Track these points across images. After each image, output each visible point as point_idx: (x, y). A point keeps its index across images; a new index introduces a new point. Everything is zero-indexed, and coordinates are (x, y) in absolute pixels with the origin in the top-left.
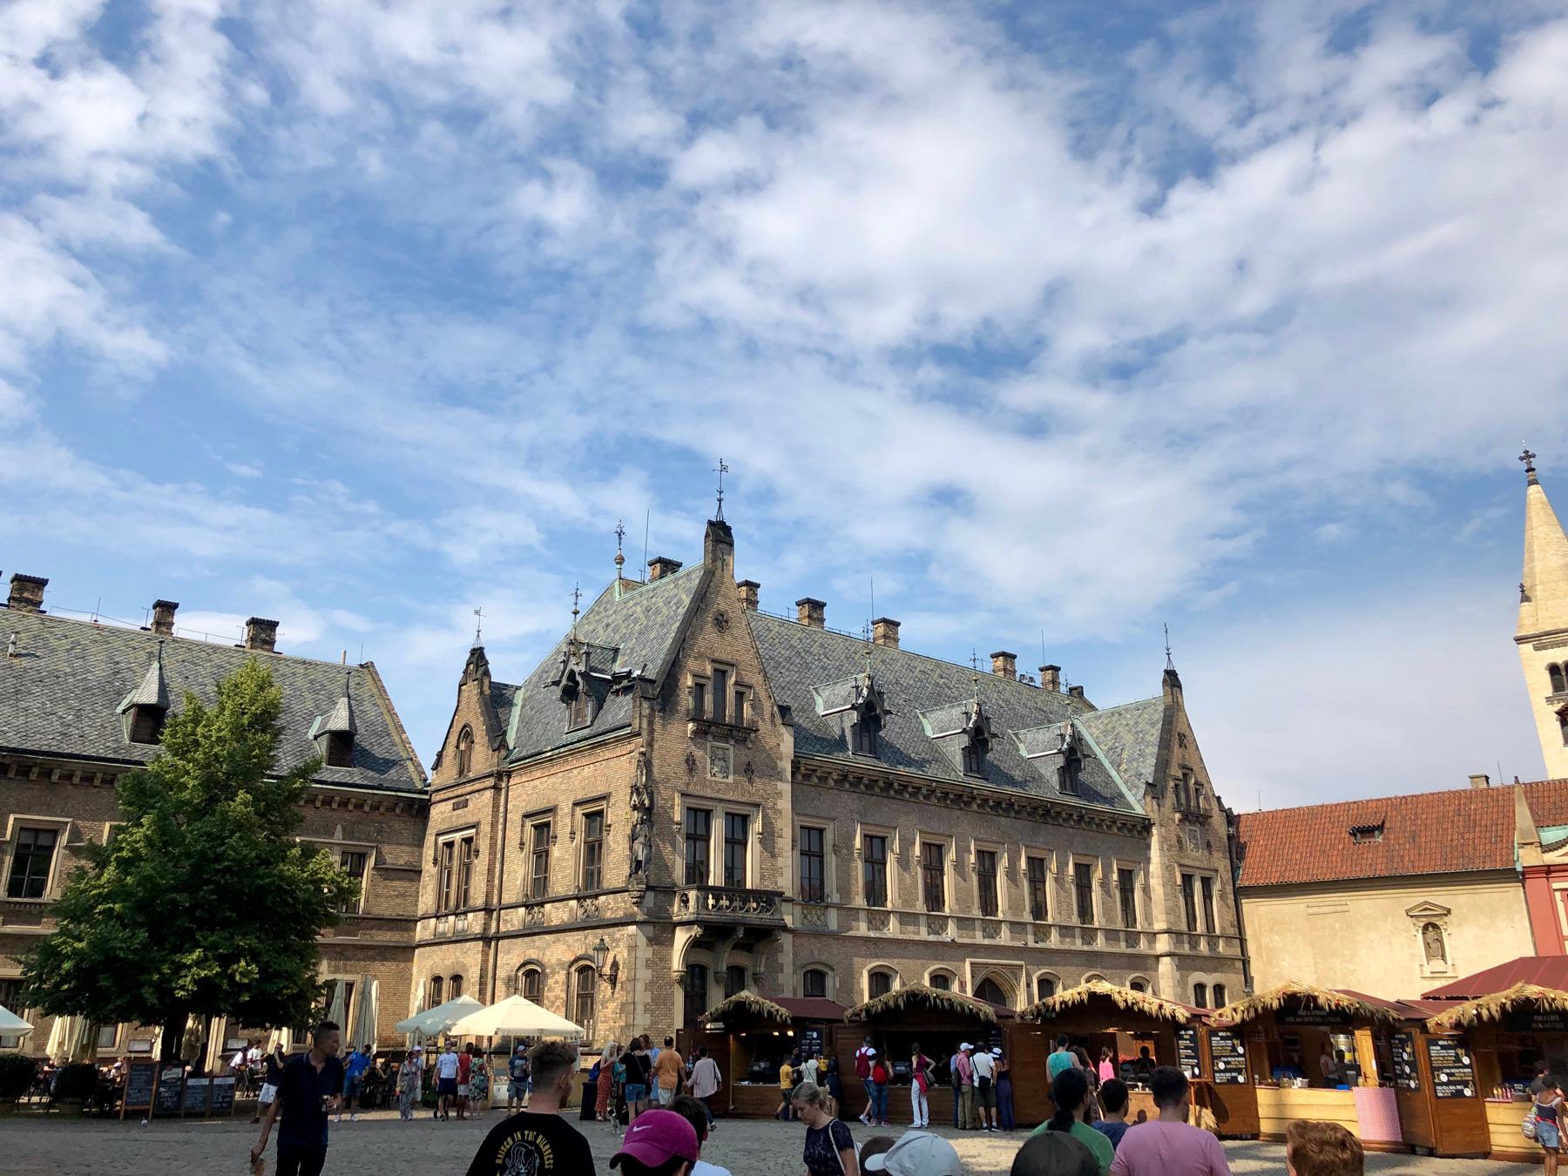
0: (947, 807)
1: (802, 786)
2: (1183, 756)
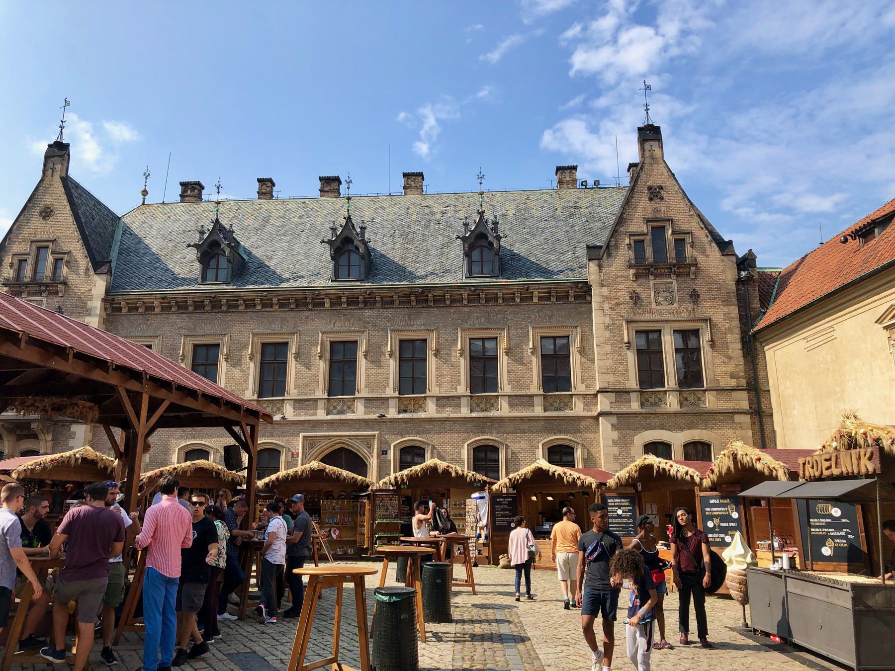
0: (292, 310)
1: (129, 317)
2: (656, 210)
